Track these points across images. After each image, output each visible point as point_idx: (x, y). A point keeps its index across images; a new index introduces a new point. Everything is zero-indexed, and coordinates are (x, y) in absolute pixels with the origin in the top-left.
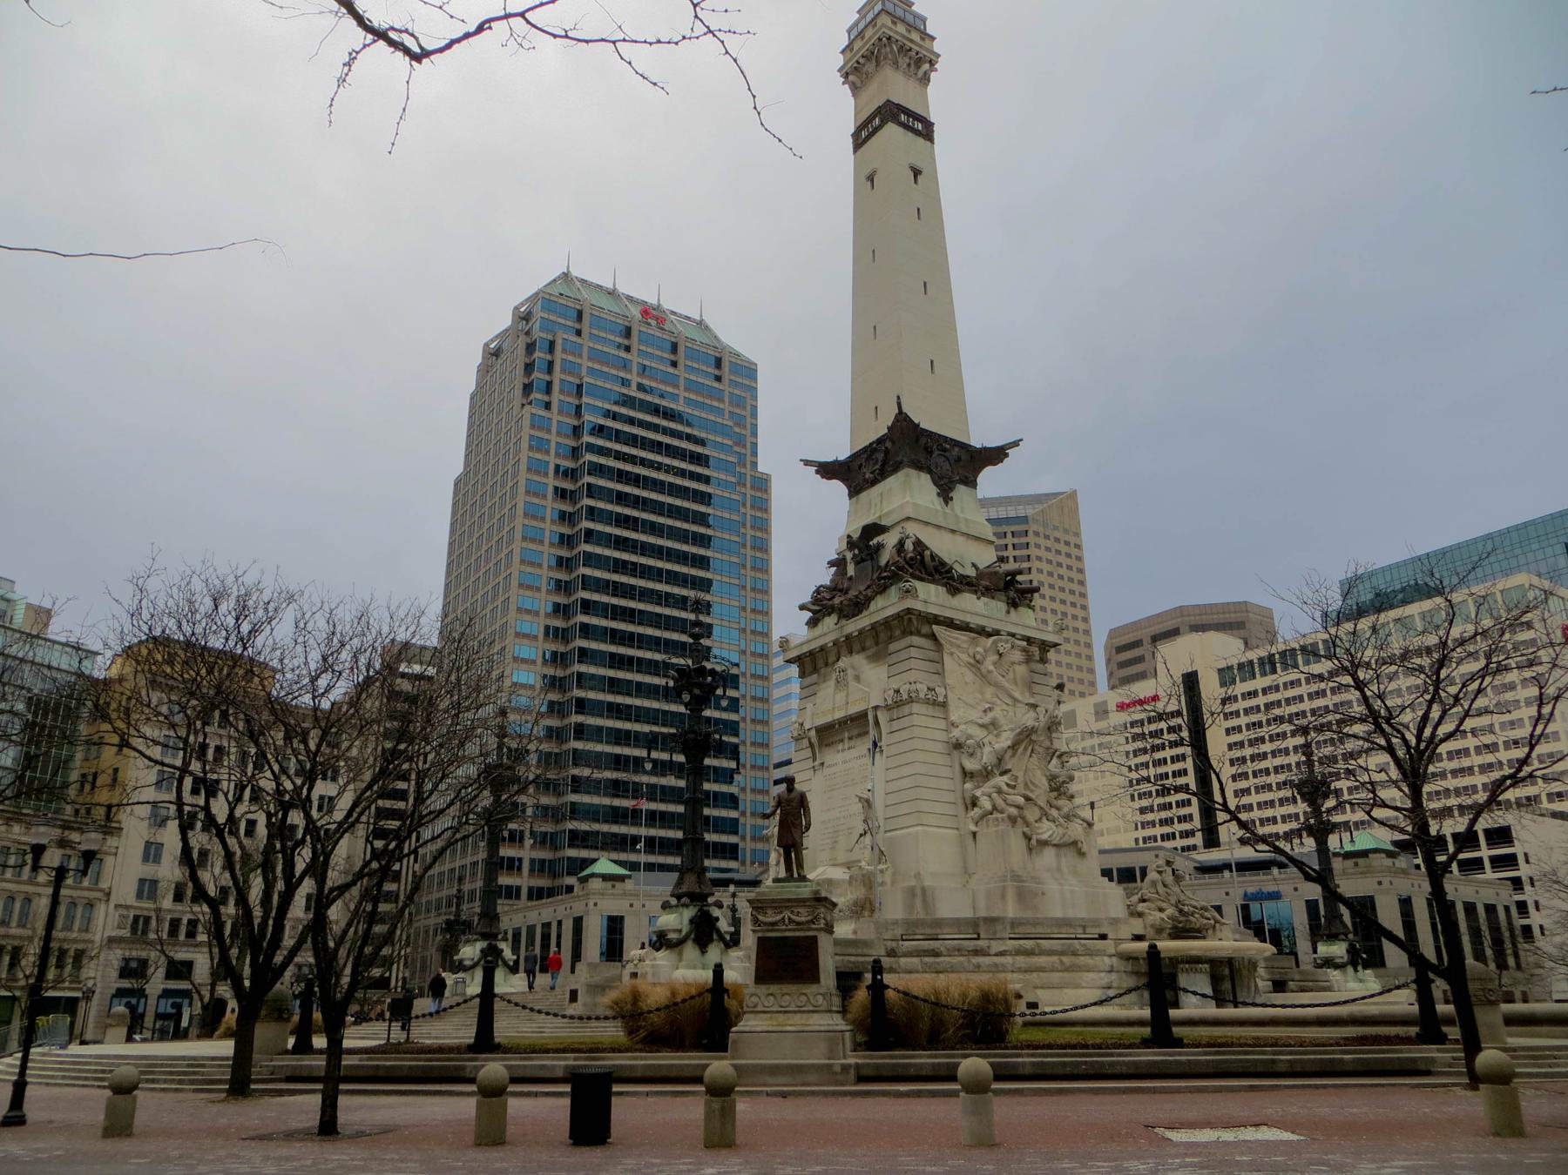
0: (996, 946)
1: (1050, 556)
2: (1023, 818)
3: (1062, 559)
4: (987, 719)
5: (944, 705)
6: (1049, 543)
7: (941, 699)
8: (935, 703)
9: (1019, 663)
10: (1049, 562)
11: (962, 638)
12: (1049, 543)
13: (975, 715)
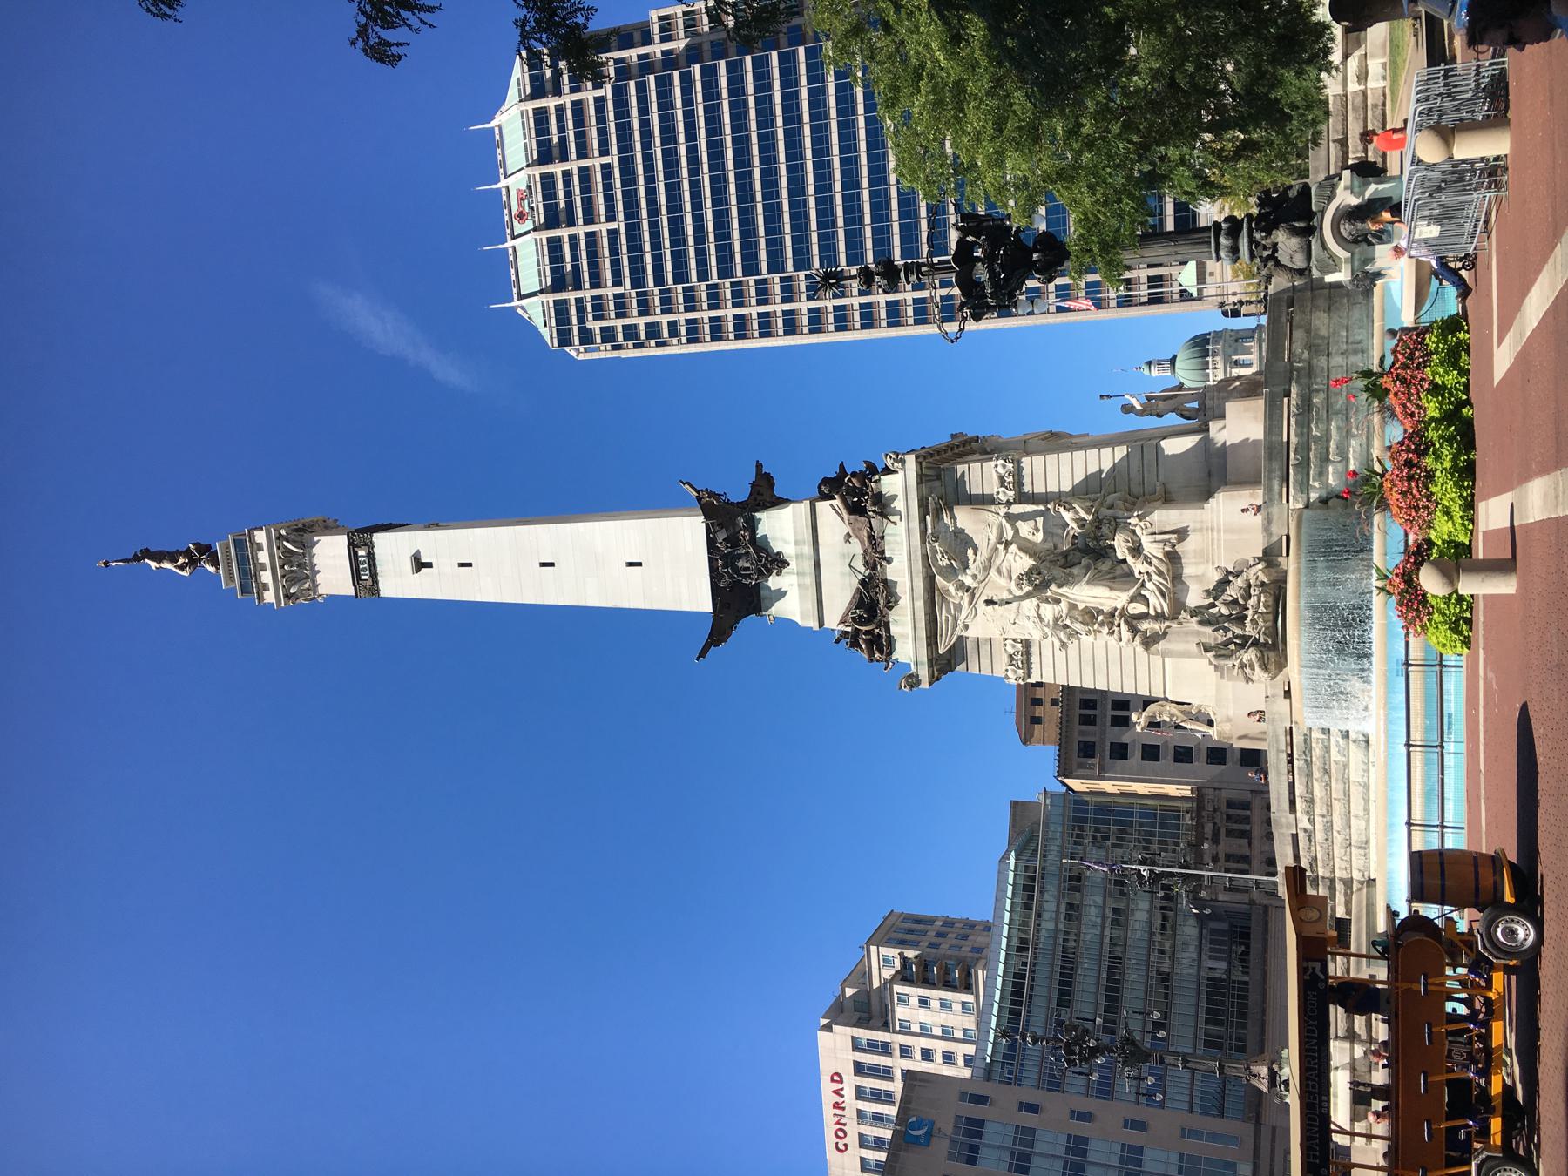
5: (1027, 644)
9: (953, 518)
11: (943, 616)
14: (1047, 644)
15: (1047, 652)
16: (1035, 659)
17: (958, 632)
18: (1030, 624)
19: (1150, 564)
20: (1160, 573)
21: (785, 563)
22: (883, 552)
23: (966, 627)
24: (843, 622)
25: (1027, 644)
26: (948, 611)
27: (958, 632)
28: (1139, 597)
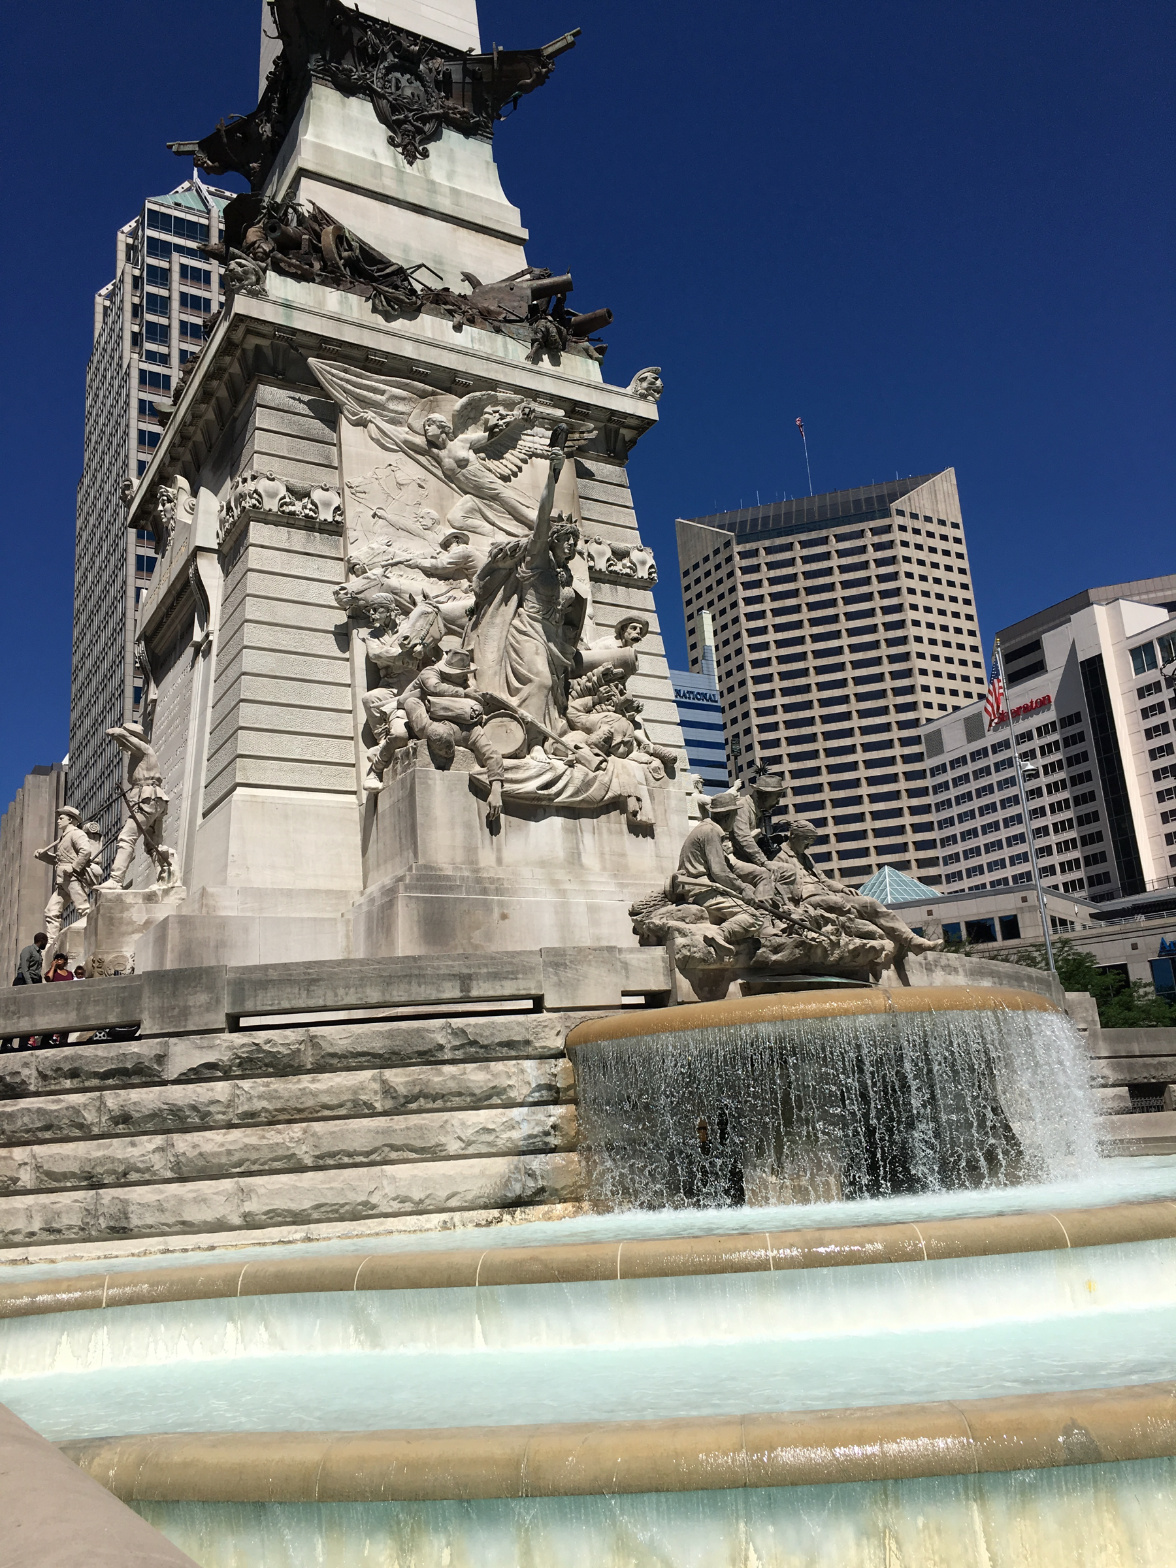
0: (185, 1055)
1: (921, 555)
2: (474, 748)
3: (938, 558)
4: (445, 559)
5: (335, 529)
6: (919, 539)
7: (326, 515)
8: (310, 525)
10: (921, 563)
11: (387, 389)
12: (919, 539)
13: (425, 551)
14: (336, 571)
15: (311, 568)
16: (298, 539)
17: (351, 405)
18: (378, 543)
19: (598, 768)
20: (587, 784)
21: (411, 158)
22: (472, 322)
23: (362, 423)
24: (321, 217)
25: (335, 529)
26: (394, 398)
27: (351, 405)
28: (535, 737)
